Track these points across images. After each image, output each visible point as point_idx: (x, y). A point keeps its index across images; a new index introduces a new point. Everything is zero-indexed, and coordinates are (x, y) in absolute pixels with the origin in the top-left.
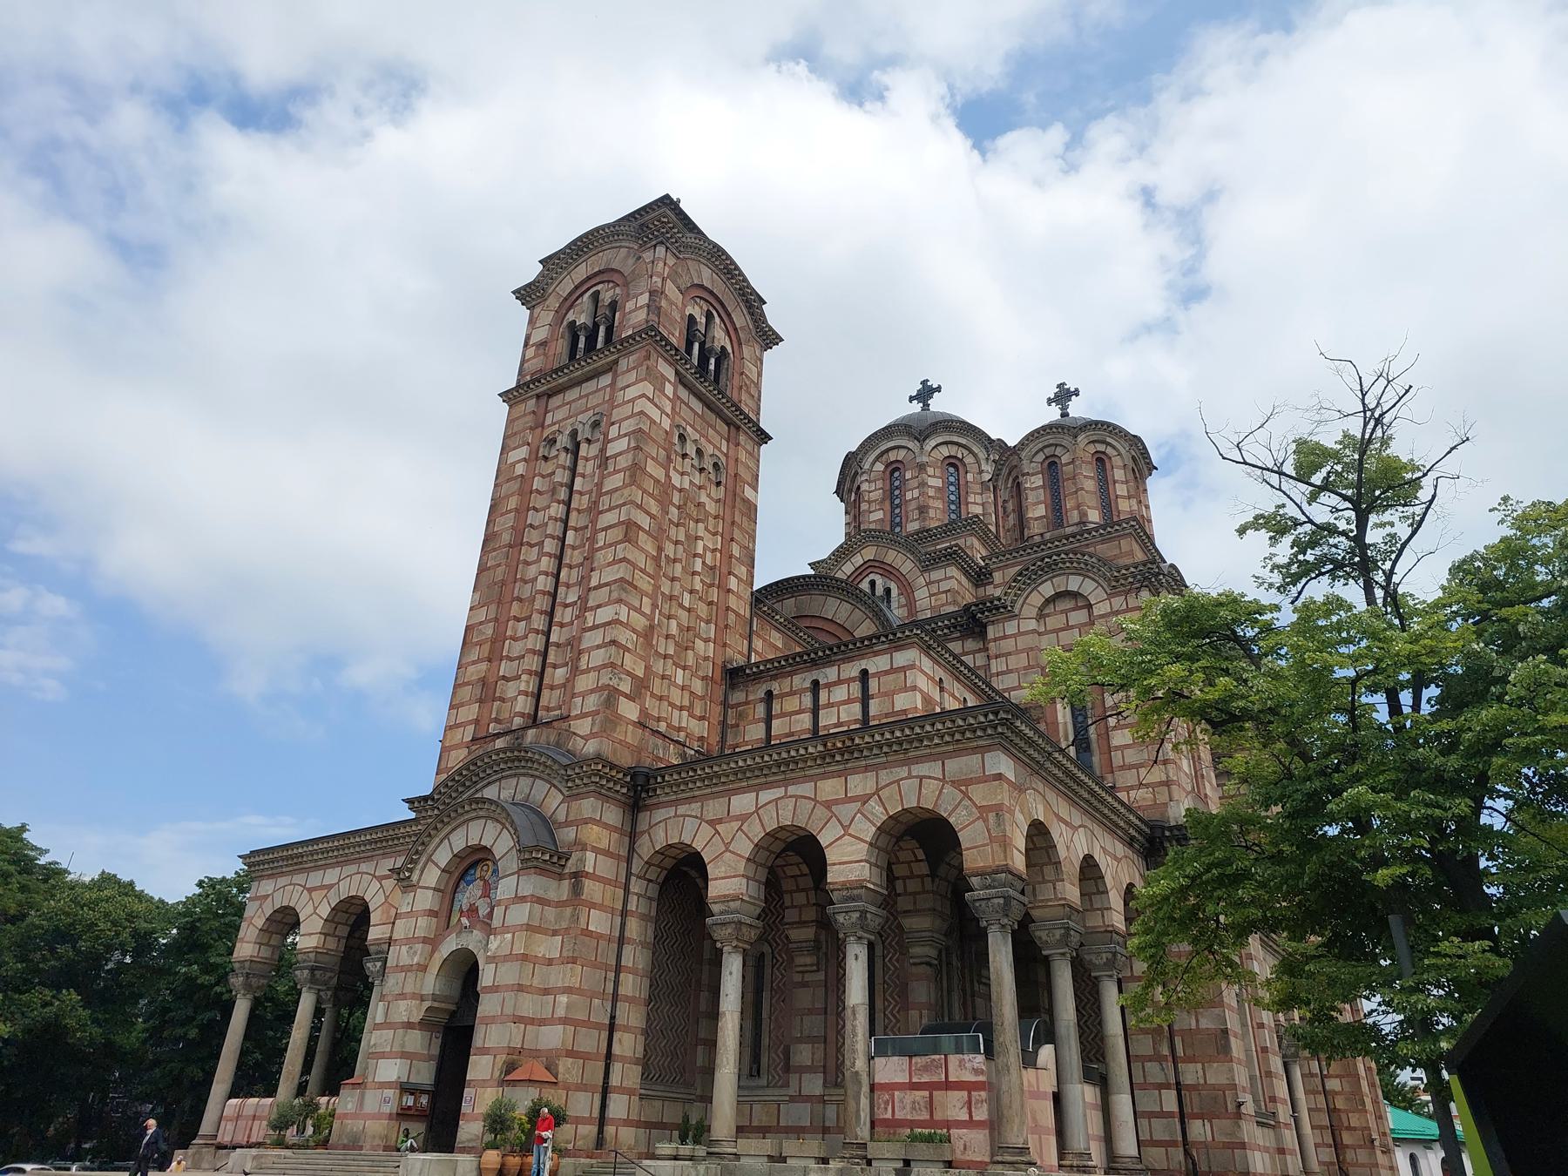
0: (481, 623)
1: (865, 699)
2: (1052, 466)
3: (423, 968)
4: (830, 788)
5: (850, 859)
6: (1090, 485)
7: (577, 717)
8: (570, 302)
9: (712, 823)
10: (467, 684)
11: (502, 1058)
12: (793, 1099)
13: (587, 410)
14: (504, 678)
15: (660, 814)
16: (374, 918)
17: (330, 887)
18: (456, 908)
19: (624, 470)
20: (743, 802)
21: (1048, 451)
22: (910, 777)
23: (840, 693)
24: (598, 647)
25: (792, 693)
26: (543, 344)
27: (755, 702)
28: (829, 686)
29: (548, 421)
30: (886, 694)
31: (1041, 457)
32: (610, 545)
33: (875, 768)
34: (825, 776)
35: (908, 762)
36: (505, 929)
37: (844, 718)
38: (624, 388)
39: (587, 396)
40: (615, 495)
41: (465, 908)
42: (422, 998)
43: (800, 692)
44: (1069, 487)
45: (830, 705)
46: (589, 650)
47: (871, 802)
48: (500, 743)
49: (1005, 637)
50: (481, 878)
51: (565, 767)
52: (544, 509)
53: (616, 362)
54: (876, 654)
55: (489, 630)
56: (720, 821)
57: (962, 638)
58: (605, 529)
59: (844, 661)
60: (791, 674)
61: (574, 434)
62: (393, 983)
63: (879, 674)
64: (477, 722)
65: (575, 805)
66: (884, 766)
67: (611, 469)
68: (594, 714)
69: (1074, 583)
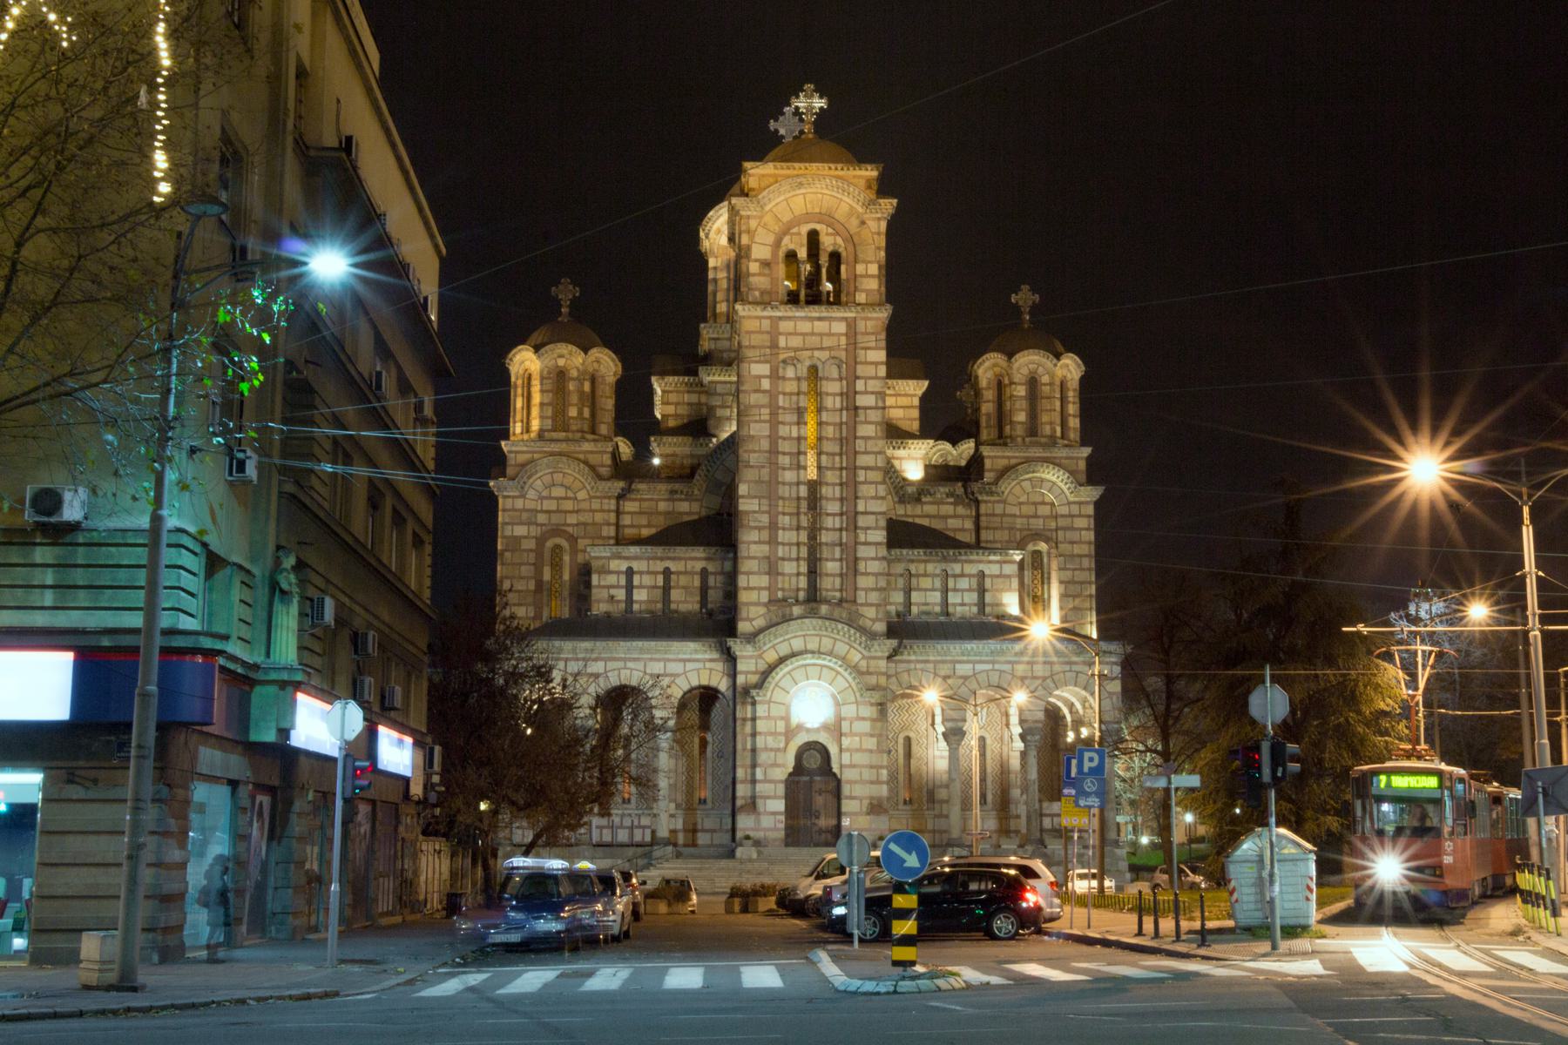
6: (1058, 404)
11: (866, 802)
13: (822, 349)
14: (783, 559)
15: (902, 666)
17: (597, 676)
19: (876, 423)
23: (964, 583)
25: (925, 575)
26: (766, 264)
27: (896, 575)
28: (955, 576)
29: (782, 342)
31: (1025, 371)
36: (852, 734)
37: (967, 600)
38: (866, 349)
39: (821, 335)
40: (870, 443)
44: (1045, 404)
45: (955, 590)
46: (866, 559)
48: (797, 610)
52: (790, 424)
55: (765, 519)
57: (955, 504)
58: (866, 468)
60: (925, 562)
61: (813, 370)
62: (763, 757)
64: (768, 589)
65: (873, 663)
67: (861, 418)
68: (877, 606)
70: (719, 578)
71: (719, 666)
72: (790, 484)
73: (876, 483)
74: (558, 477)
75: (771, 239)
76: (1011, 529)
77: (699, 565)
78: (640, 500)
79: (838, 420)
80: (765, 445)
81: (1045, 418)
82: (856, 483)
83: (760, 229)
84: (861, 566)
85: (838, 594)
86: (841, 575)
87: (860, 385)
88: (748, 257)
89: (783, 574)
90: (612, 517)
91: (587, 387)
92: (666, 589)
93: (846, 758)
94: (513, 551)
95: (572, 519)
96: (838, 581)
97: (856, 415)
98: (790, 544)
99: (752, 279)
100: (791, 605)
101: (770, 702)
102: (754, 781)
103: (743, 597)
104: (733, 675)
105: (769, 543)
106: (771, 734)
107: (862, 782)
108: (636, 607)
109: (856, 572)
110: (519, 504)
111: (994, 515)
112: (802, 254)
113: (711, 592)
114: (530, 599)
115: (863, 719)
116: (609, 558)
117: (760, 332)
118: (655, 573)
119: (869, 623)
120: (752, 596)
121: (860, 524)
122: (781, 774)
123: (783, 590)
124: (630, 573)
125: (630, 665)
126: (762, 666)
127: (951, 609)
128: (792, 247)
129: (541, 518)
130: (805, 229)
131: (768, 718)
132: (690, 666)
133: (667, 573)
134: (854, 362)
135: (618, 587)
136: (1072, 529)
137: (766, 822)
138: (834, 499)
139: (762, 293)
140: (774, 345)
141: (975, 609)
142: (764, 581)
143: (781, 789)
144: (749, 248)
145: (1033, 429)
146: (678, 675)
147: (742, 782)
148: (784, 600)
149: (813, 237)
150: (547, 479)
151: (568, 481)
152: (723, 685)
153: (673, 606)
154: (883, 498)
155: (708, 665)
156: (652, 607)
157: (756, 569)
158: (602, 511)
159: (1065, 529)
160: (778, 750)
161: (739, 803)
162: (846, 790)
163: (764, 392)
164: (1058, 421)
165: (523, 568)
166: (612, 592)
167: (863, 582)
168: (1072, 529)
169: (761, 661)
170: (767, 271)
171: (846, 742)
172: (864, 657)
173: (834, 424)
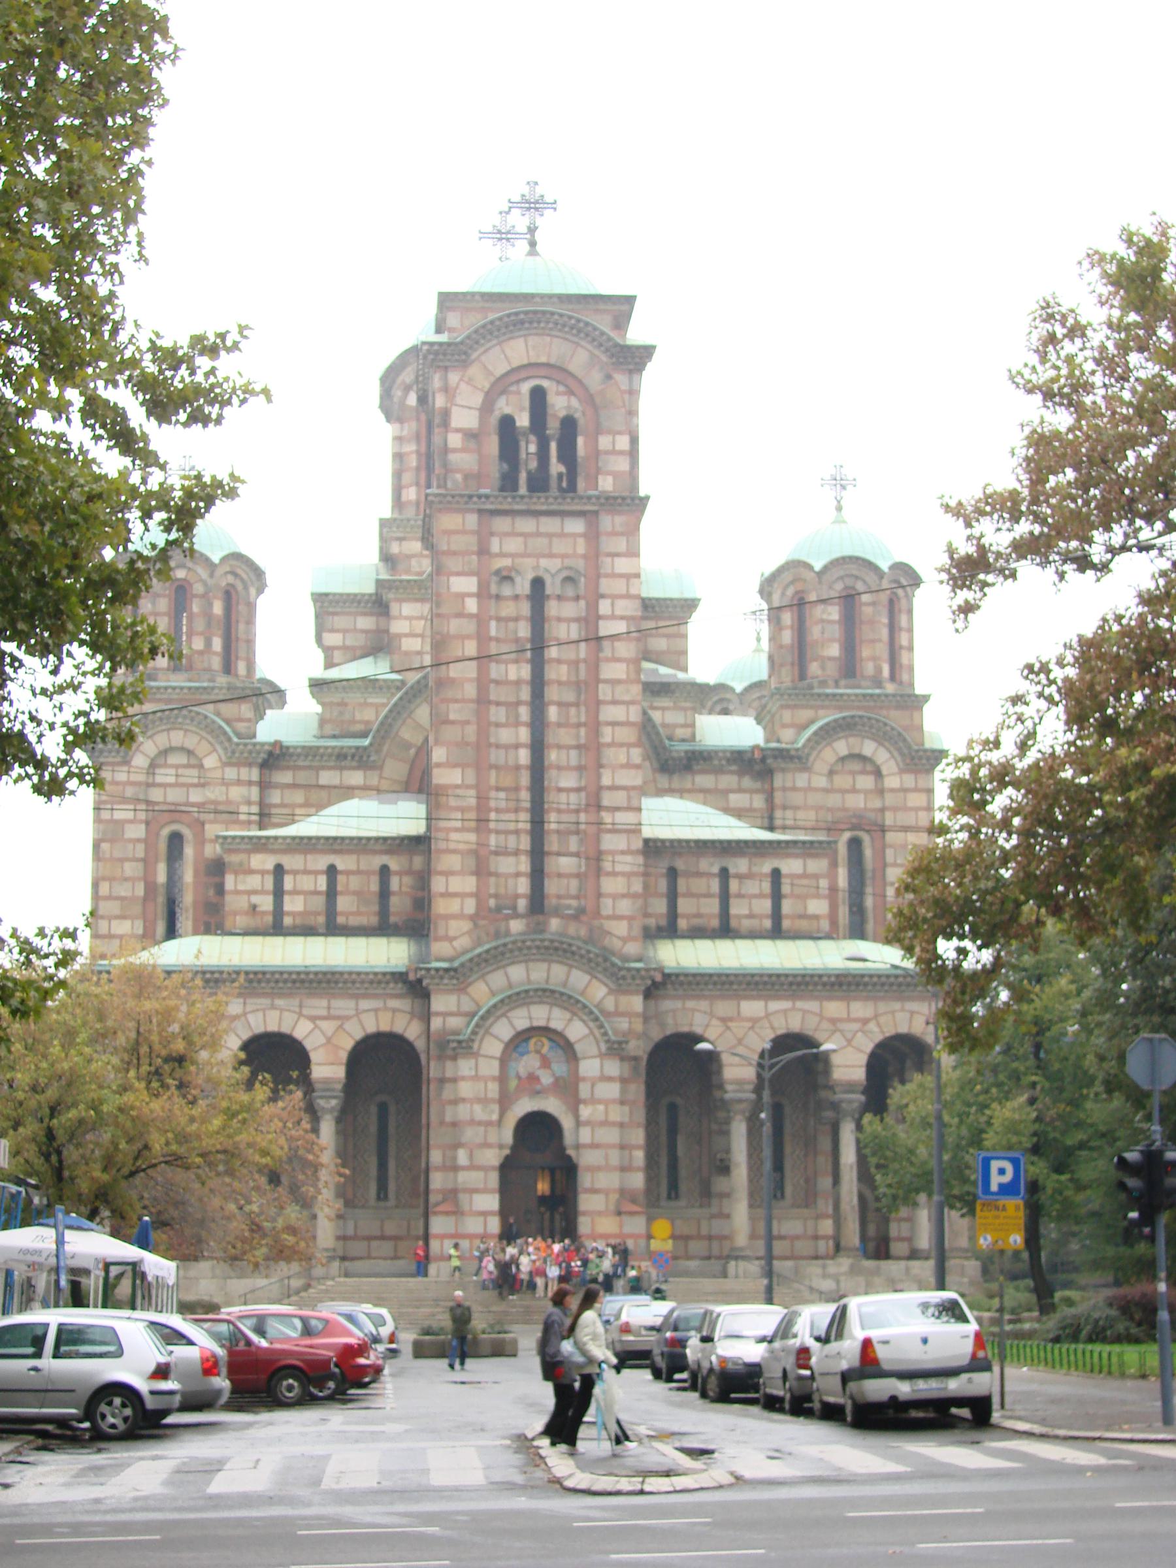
0: (457, 787)
1: (777, 896)
2: (849, 600)
3: (500, 1122)
4: (835, 1008)
5: (849, 1064)
6: (885, 632)
7: (609, 918)
8: (501, 386)
9: (724, 1020)
10: (454, 851)
11: (614, 1197)
12: (713, 1216)
13: (551, 556)
15: (667, 1005)
16: (314, 1057)
18: (512, 1073)
20: (752, 1008)
21: (849, 582)
22: (902, 1010)
23: (752, 887)
24: (623, 853)
25: (699, 874)
28: (740, 877)
29: (495, 545)
30: (798, 897)
31: (839, 586)
32: (621, 745)
33: (875, 999)
34: (830, 999)
35: (901, 999)
36: (593, 1101)
39: (550, 536)
40: (619, 689)
41: (523, 1073)
42: (501, 1147)
43: (709, 875)
44: (866, 632)
45: (740, 896)
46: (613, 853)
47: (872, 1026)
48: (516, 926)
49: (794, 789)
50: (538, 1052)
51: (620, 969)
53: (596, 513)
54: (788, 856)
56: (731, 1019)
57: (741, 774)
58: (614, 724)
59: (755, 855)
61: (538, 584)
62: (470, 1135)
63: (793, 876)
64: (477, 895)
66: (883, 999)
67: (607, 652)
68: (630, 919)
69: (869, 748)
70: (407, 880)
71: (404, 1004)
72: (507, 747)
73: (629, 745)
74: (177, 738)
75: (478, 399)
76: (817, 808)
77: (377, 861)
78: (296, 768)
79: (572, 656)
80: (471, 691)
81: (866, 652)
82: (599, 747)
83: (463, 386)
84: (607, 866)
85: (574, 903)
86: (578, 876)
87: (604, 607)
88: (445, 423)
89: (497, 875)
90: (255, 792)
91: (218, 608)
92: (331, 894)
93: (585, 1135)
94: (112, 841)
95: (196, 796)
96: (574, 884)
97: (600, 649)
98: (507, 832)
99: (453, 457)
100: (508, 918)
101: (476, 1055)
102: (455, 1168)
103: (441, 907)
104: (426, 1017)
105: (477, 830)
106: (479, 1100)
107: (607, 1168)
108: (287, 921)
109: (599, 872)
110: (122, 777)
111: (794, 789)
112: (523, 420)
113: (394, 901)
114: (137, 909)
115: (610, 1079)
116: (249, 852)
117: (464, 532)
118: (316, 873)
119: (617, 944)
120: (454, 906)
121: (605, 802)
122: (493, 1157)
123: (496, 896)
124: (279, 871)
125: (279, 1002)
126: (467, 1005)
127: (733, 923)
128: (508, 410)
129: (156, 795)
130: (526, 387)
131: (476, 1078)
132: (365, 1004)
133: (332, 871)
134: (597, 576)
135: (263, 892)
136: (906, 809)
137: (473, 1225)
138: (568, 768)
139: (466, 477)
140: (483, 551)
141: (768, 924)
142: (469, 884)
143: (494, 1179)
144: (446, 414)
145: (849, 667)
146: (348, 1018)
147: (437, 1169)
148: (498, 909)
149: (538, 397)
150: (162, 740)
151: (191, 742)
152: (412, 1031)
153: (341, 920)
154: (638, 767)
155: (394, 1003)
156: (311, 921)
157: (458, 867)
158: (239, 782)
159: (895, 809)
160: (489, 1124)
161: (433, 1198)
162: (585, 1180)
163: (470, 616)
164: (885, 655)
165: (127, 865)
166: (255, 899)
167: (610, 885)
168: (906, 809)
169: (464, 999)
170: (472, 445)
171: (585, 1112)
172: (611, 992)
173: (569, 663)
